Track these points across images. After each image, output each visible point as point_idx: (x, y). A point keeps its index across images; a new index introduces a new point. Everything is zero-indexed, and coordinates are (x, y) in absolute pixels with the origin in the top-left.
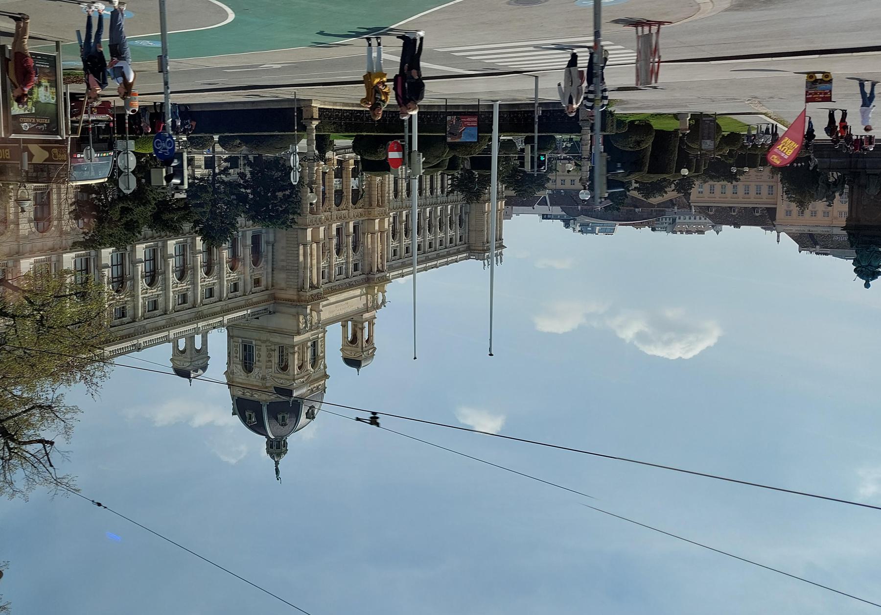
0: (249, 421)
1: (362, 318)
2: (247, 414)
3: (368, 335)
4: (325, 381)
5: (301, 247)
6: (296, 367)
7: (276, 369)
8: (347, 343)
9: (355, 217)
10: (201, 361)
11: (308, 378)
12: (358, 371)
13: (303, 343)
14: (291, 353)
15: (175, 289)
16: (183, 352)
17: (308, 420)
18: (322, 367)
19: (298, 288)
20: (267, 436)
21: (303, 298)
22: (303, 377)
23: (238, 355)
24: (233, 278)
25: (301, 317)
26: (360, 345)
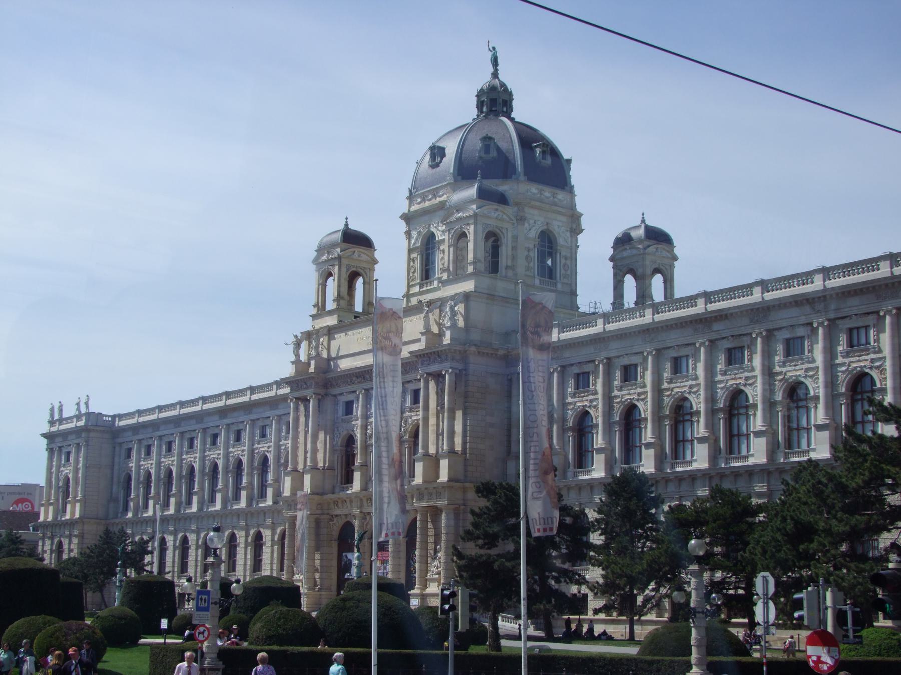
0: (545, 149)
1: (339, 316)
3: (326, 286)
4: (409, 211)
5: (458, 448)
6: (471, 237)
7: (505, 235)
8: (366, 274)
9: (348, 501)
10: (625, 254)
11: (448, 218)
12: (347, 225)
13: (457, 275)
14: (479, 261)
15: (694, 383)
16: (656, 271)
17: (441, 145)
18: (414, 234)
20: (512, 120)
23: (563, 261)
24: (584, 399)
25: (461, 323)
26: (344, 270)
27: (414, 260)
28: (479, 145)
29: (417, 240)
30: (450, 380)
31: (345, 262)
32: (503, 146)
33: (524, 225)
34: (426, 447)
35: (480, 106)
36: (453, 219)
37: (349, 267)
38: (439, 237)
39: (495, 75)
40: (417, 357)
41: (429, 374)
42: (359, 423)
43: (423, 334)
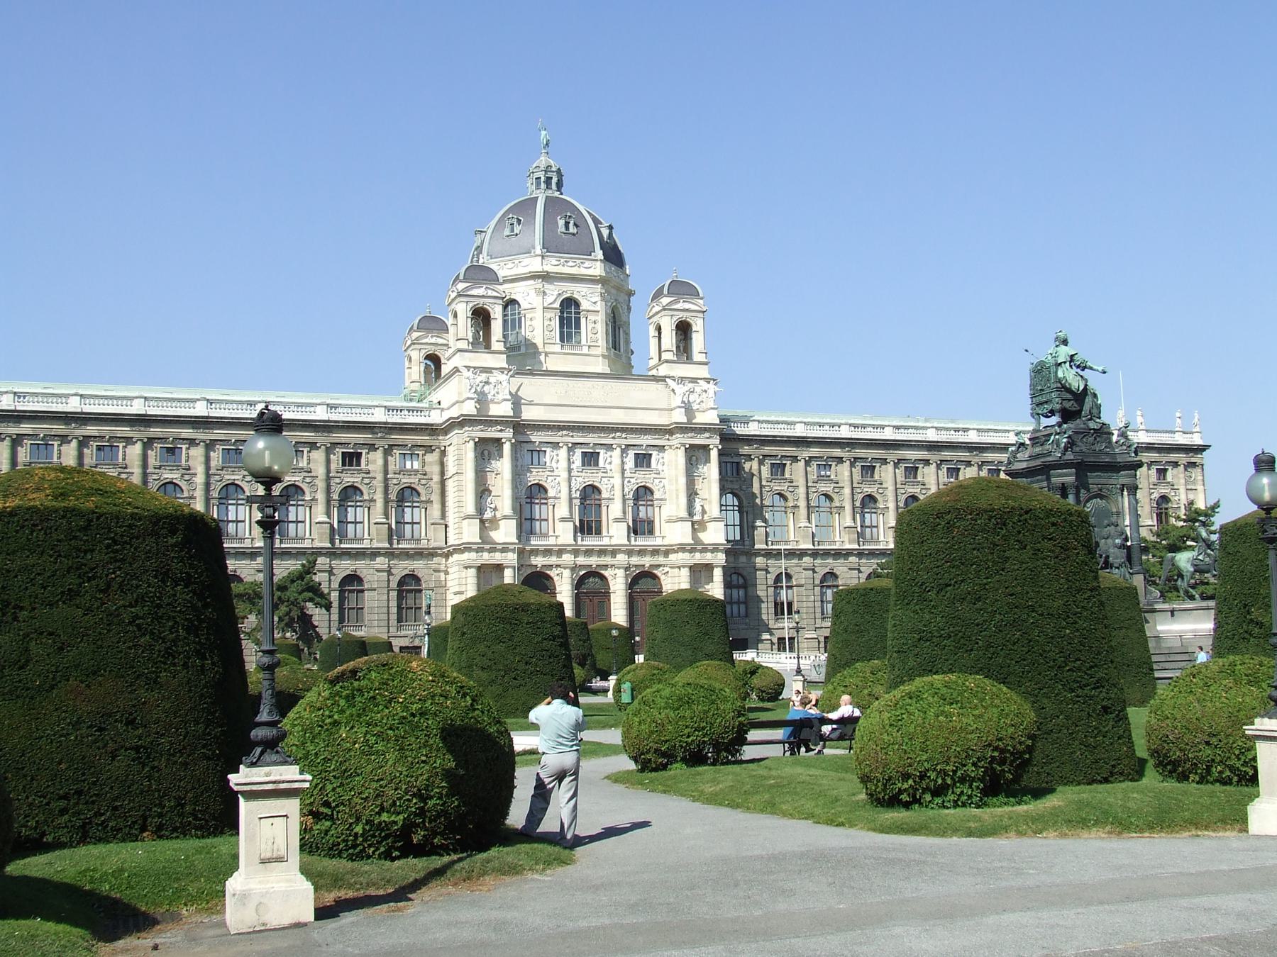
29: (555, 300)
38: (585, 305)
42: (565, 475)
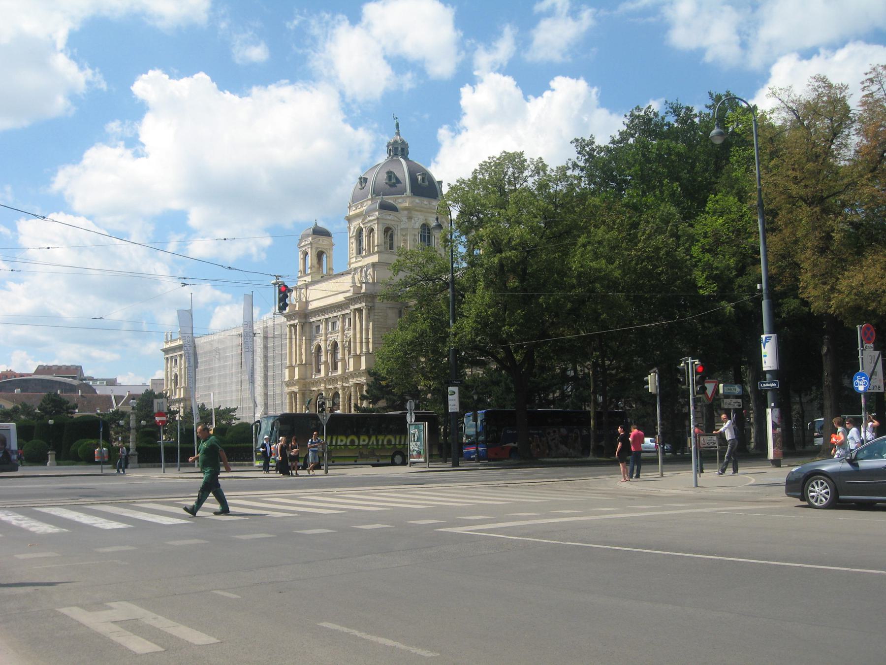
2: (427, 183)
13: (370, 254)
19: (374, 309)
21: (369, 300)
22: (370, 221)
26: (314, 250)
27: (352, 244)
28: (386, 176)
30: (366, 313)
31: (315, 246)
32: (399, 175)
33: (411, 221)
34: (355, 350)
35: (389, 151)
36: (366, 221)
37: (317, 248)
39: (398, 134)
40: (348, 300)
41: (355, 310)
42: (323, 338)
43: (351, 287)
